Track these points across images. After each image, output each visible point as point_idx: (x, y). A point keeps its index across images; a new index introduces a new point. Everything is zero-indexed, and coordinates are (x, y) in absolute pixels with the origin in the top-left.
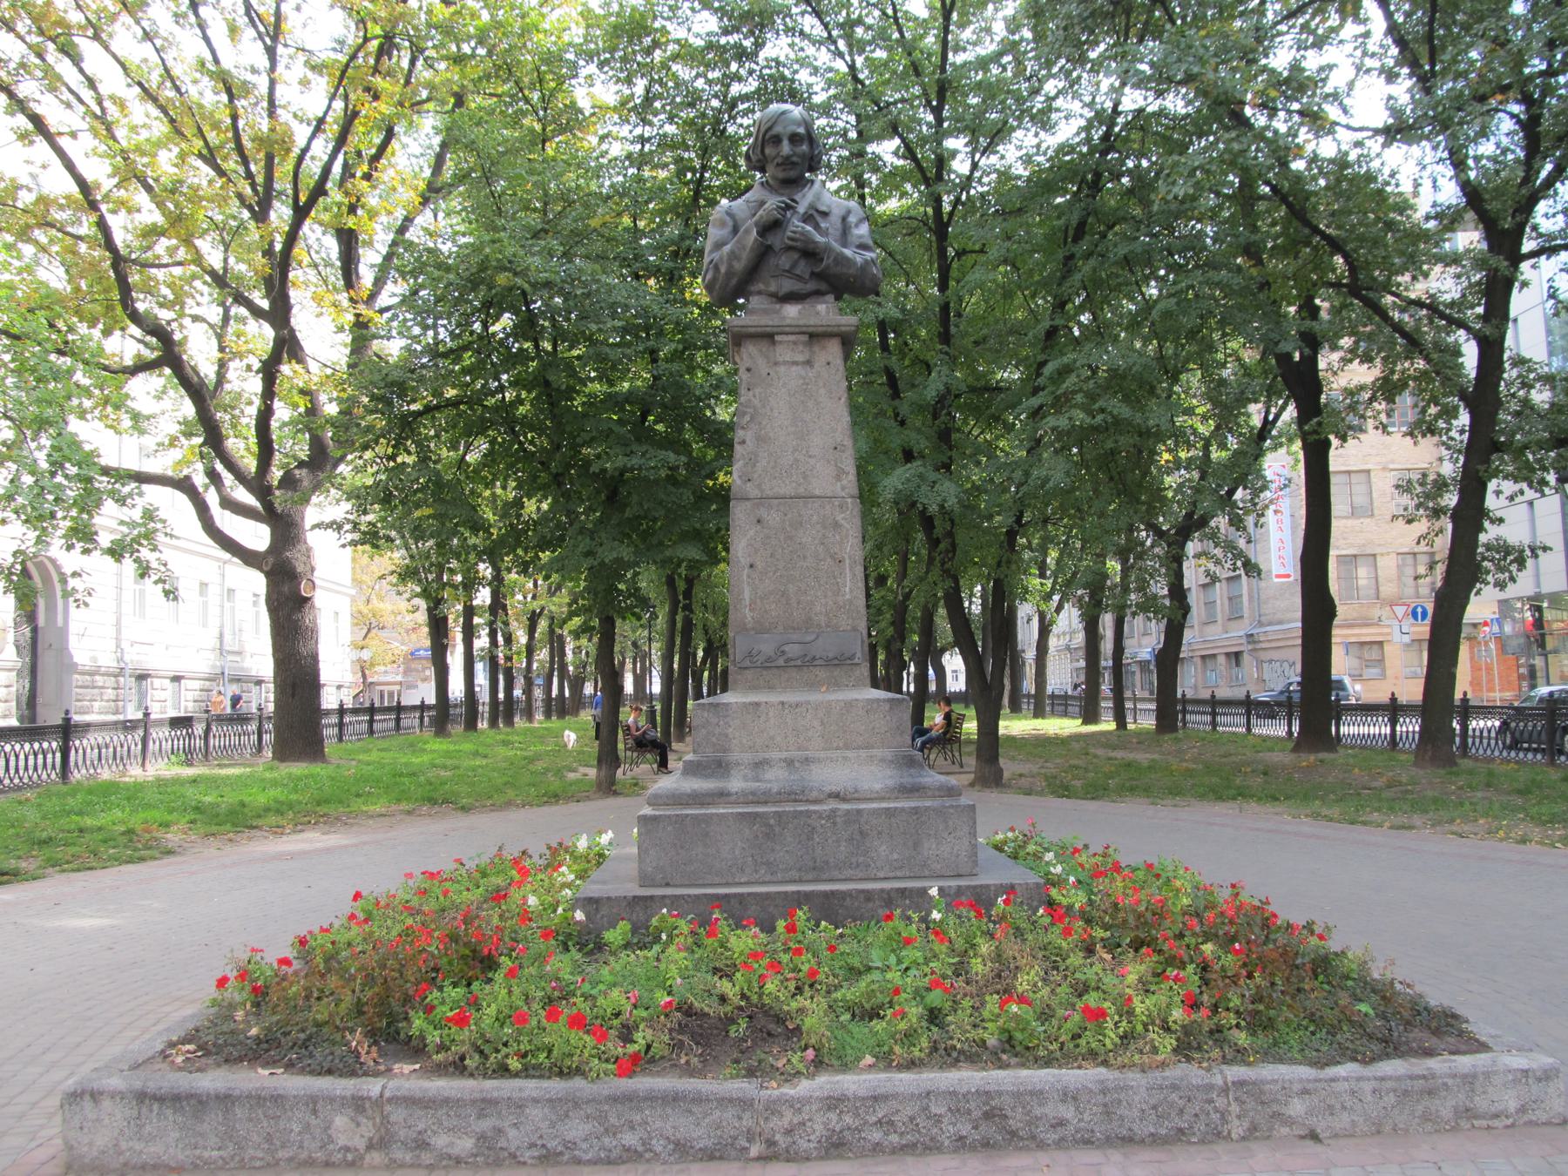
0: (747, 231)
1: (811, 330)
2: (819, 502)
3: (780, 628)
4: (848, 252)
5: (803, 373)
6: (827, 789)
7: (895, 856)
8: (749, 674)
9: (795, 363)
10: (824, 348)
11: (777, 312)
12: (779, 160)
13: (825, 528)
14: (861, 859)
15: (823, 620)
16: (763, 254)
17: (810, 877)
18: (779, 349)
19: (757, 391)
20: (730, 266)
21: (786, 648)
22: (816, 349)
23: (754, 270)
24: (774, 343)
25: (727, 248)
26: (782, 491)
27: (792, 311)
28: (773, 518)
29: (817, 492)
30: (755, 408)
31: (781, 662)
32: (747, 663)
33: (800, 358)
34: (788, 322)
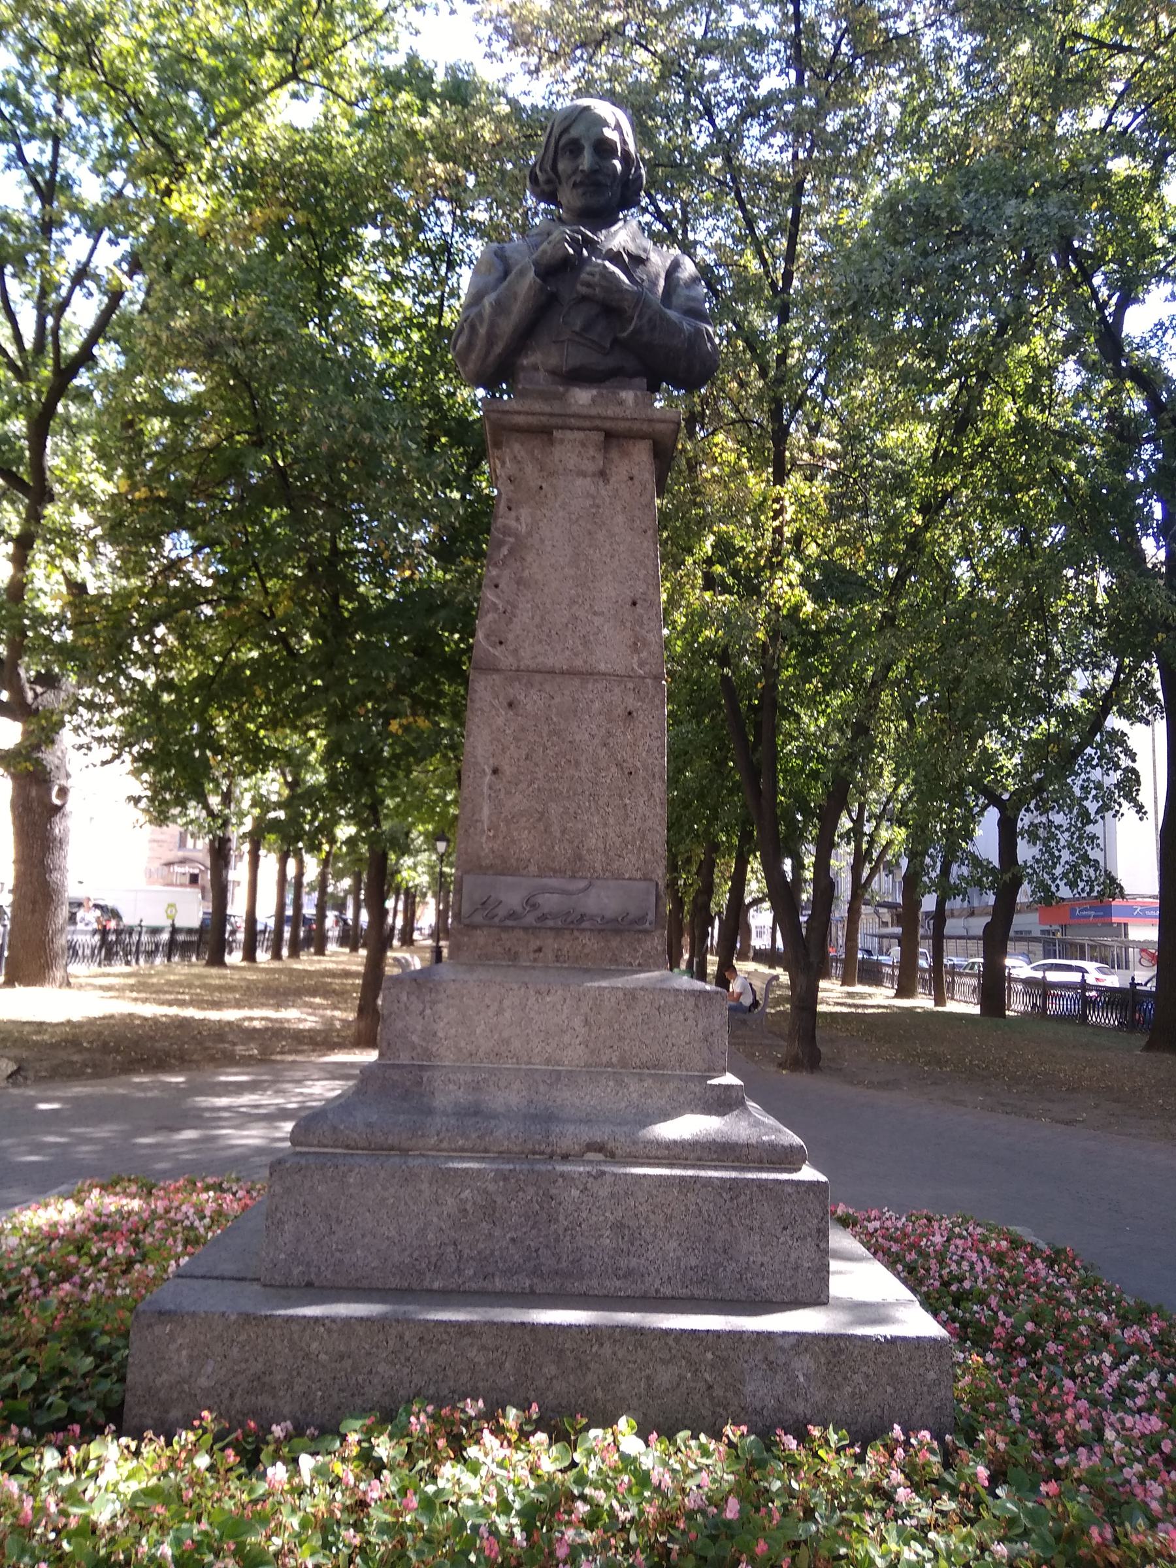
0: (522, 273)
1: (608, 425)
2: (600, 686)
3: (533, 869)
4: (672, 314)
5: (593, 490)
6: (587, 1134)
7: (693, 1262)
8: (481, 937)
9: (584, 474)
10: (625, 454)
11: (561, 397)
12: (578, 178)
13: (610, 721)
14: (634, 1262)
15: (599, 860)
16: (544, 309)
17: (550, 1287)
18: (558, 452)
19: (524, 513)
20: (493, 325)
21: (540, 899)
22: (614, 454)
23: (527, 334)
24: (551, 442)
25: (488, 301)
26: (550, 661)
27: (582, 397)
28: (532, 701)
29: (602, 667)
30: (516, 535)
31: (530, 919)
32: (478, 918)
33: (590, 467)
34: (574, 409)
